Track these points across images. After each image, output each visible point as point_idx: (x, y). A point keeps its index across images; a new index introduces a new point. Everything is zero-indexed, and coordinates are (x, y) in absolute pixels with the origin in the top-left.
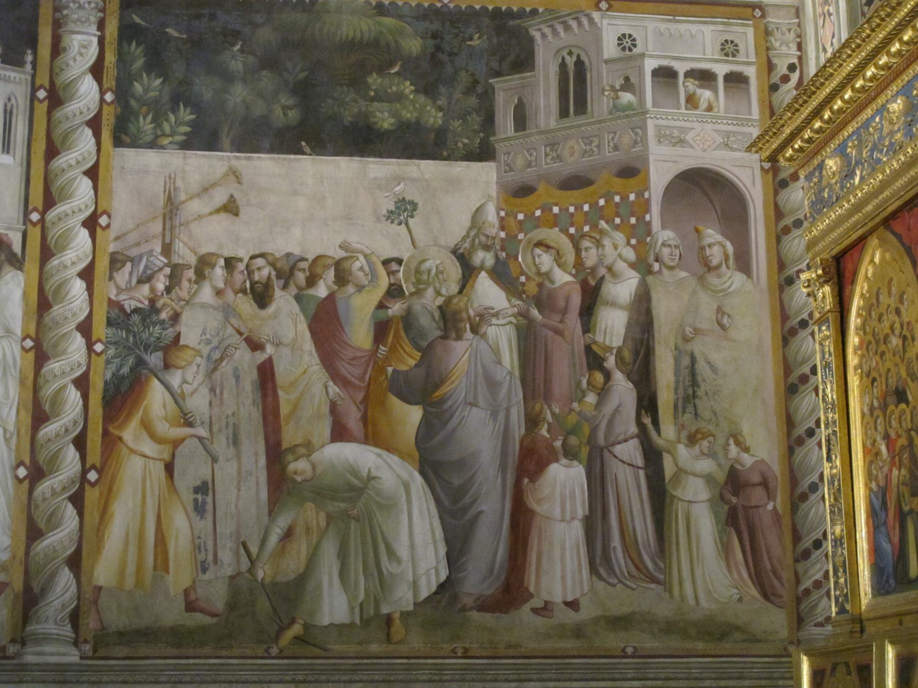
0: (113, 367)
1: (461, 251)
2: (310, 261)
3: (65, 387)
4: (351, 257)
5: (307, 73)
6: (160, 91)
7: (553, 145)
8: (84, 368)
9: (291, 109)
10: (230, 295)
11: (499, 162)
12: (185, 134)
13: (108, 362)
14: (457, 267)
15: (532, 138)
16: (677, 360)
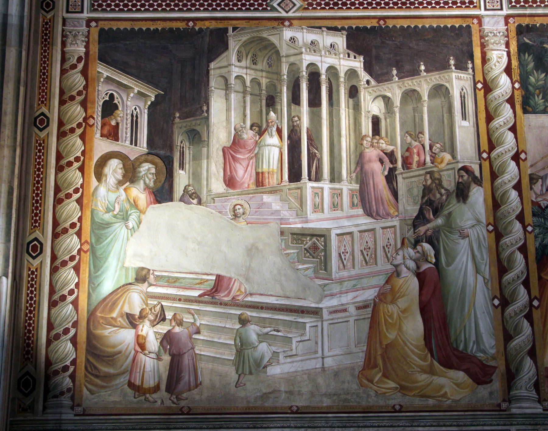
0: (540, 240)
3: (514, 252)
6: (545, 80)
8: (523, 241)
13: (536, 237)
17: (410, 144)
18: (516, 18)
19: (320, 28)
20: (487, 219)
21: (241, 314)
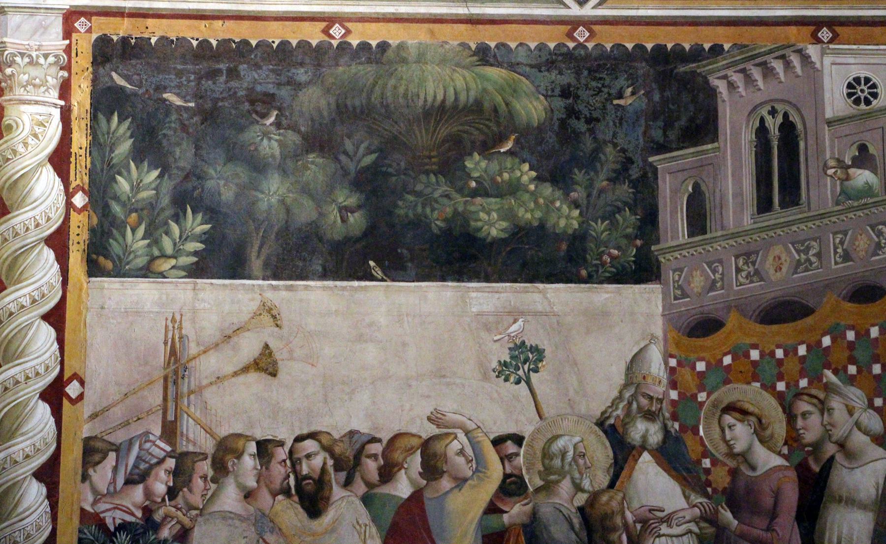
1: (612, 421)
2: (385, 442)
4: (447, 434)
5: (373, 157)
6: (156, 189)
9: (352, 212)
10: (265, 498)
11: (666, 284)
12: (196, 253)
14: (606, 448)
15: (715, 245)
18: (94, 18)
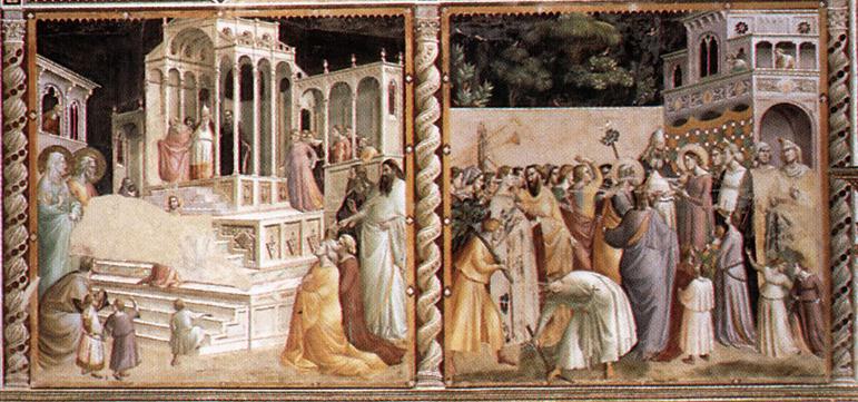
7: (698, 93)
13: (453, 229)
16: (767, 218)
17: (338, 138)
19: (253, 18)
20: (408, 210)
21: (176, 301)
